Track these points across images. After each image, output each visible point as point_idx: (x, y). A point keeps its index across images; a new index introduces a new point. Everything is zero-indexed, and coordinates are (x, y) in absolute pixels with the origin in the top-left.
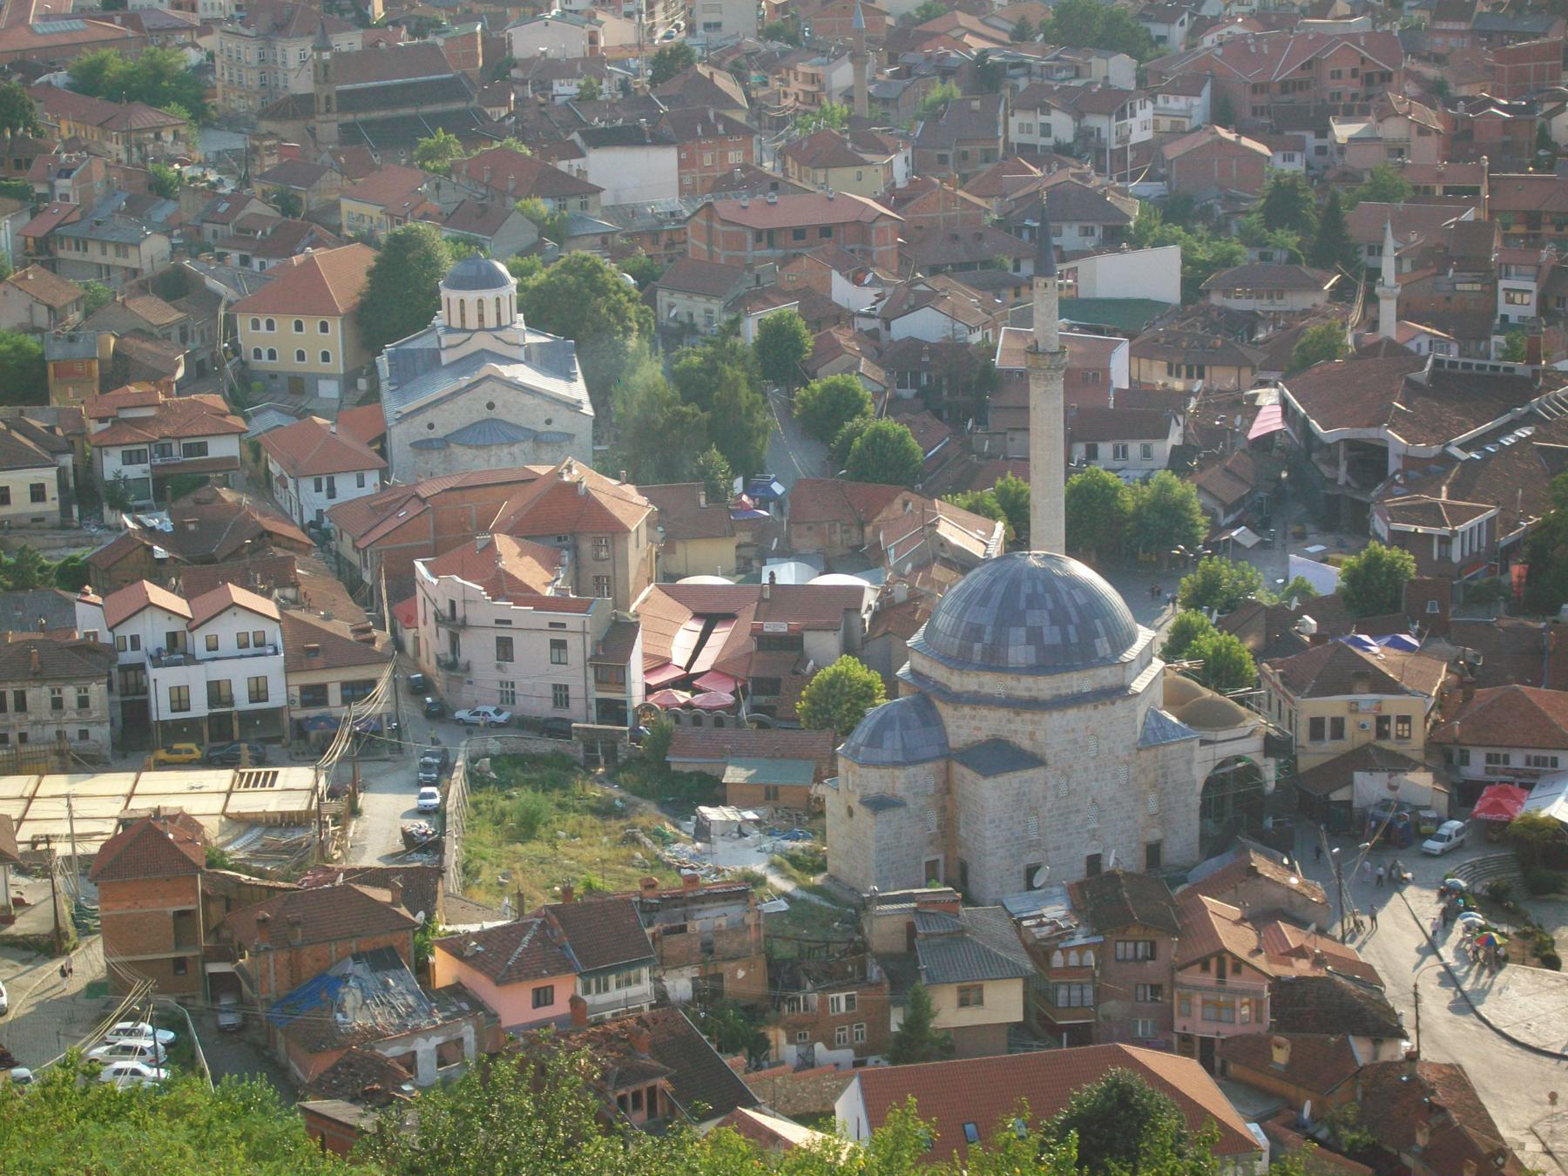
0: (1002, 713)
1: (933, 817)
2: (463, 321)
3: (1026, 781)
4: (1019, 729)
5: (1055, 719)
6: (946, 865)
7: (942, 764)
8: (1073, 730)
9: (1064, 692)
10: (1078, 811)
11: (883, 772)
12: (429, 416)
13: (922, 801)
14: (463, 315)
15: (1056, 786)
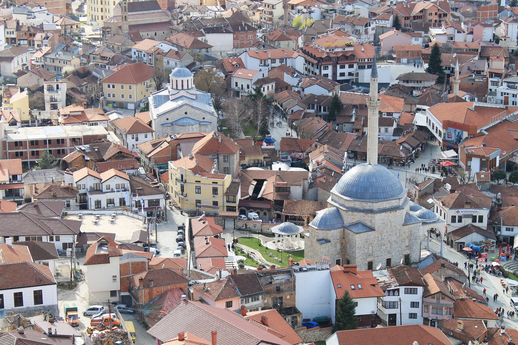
0: (362, 214)
1: (339, 246)
2: (177, 87)
3: (369, 235)
4: (366, 219)
5: (378, 216)
6: (342, 261)
7: (342, 229)
8: (384, 220)
9: (381, 207)
10: (384, 245)
11: (324, 232)
12: (167, 116)
13: (335, 241)
14: (177, 85)
15: (378, 237)
